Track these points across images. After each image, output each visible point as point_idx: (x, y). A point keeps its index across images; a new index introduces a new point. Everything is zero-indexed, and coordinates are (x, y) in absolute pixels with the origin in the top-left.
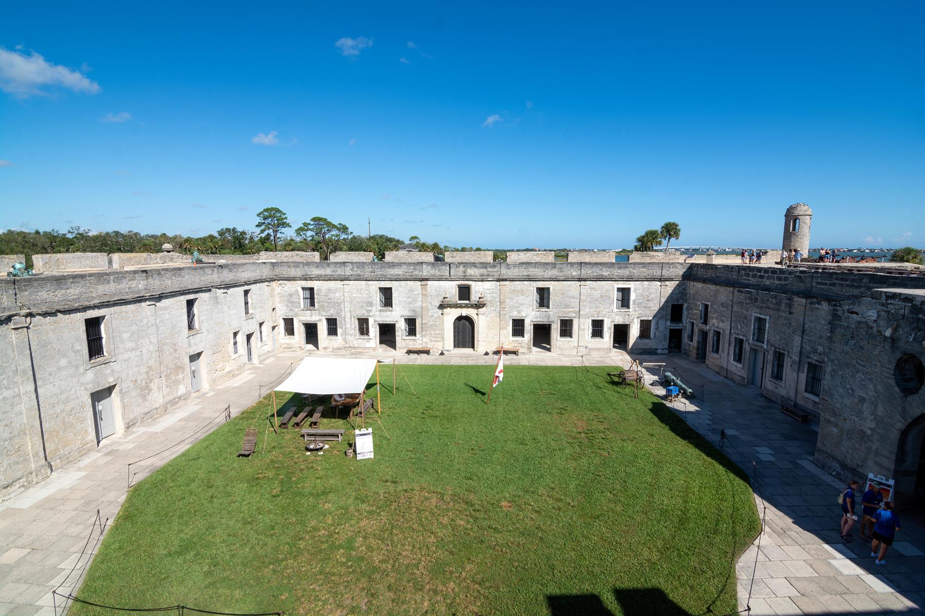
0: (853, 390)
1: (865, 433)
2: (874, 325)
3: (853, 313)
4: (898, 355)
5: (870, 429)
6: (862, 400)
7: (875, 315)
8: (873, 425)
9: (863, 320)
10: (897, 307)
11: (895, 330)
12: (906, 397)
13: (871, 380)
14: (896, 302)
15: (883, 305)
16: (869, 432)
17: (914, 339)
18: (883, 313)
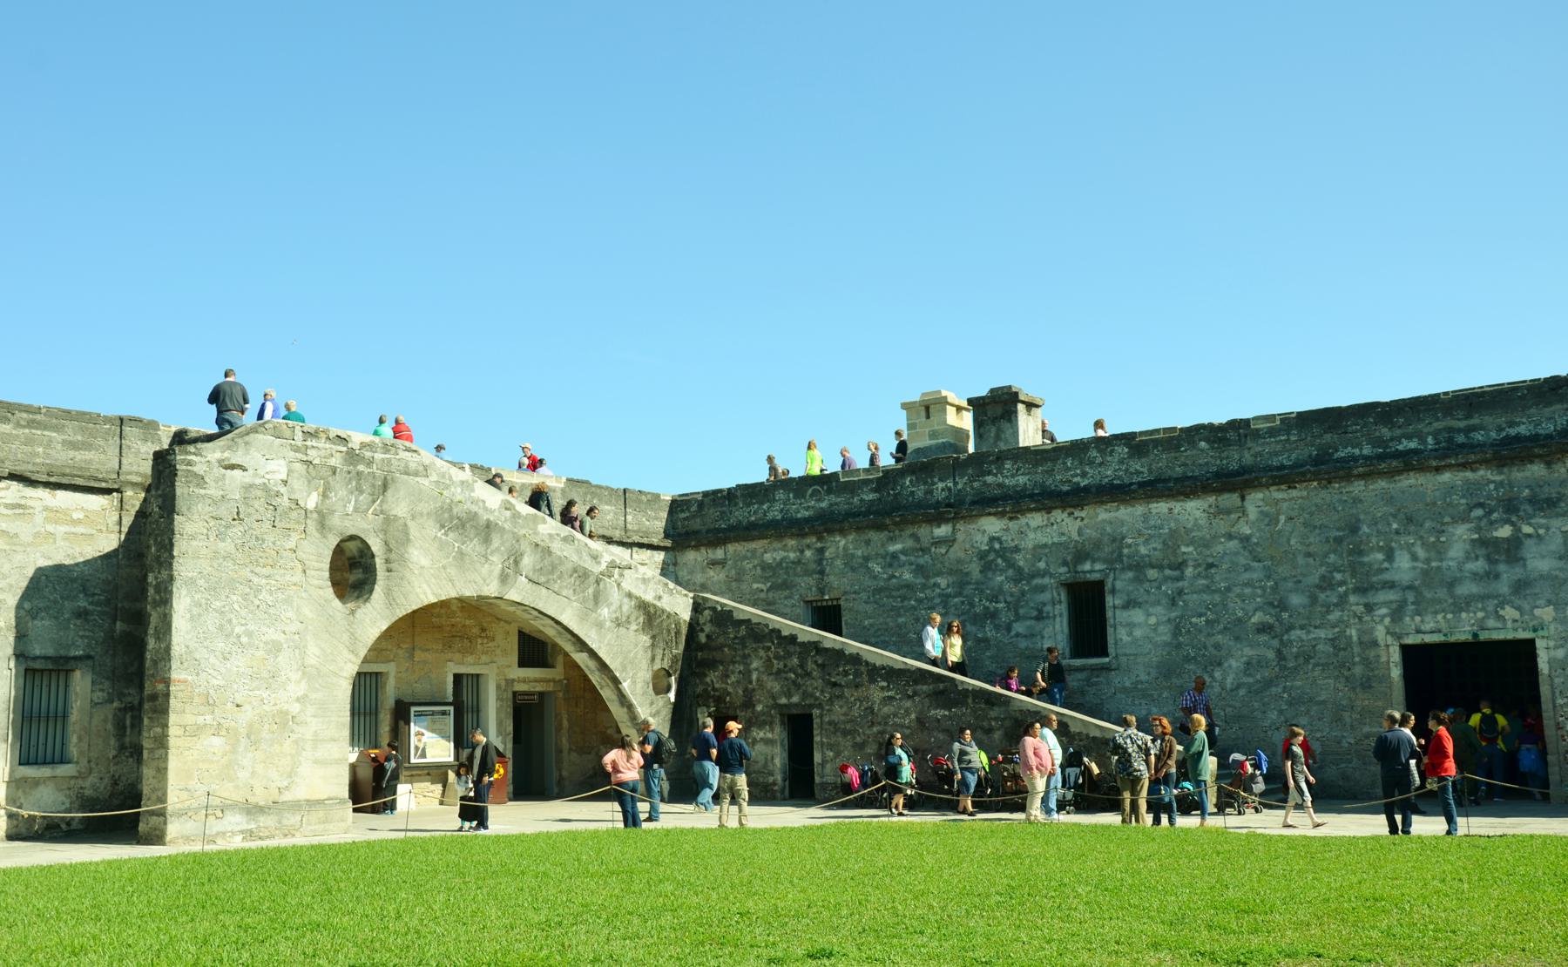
0: (249, 634)
1: (287, 713)
2: (283, 490)
3: (232, 467)
4: (333, 541)
5: (298, 700)
6: (275, 648)
7: (284, 470)
8: (301, 689)
9: (258, 481)
10: (323, 453)
11: (325, 496)
12: (353, 612)
13: (288, 601)
14: (321, 443)
15: (297, 450)
16: (295, 708)
17: (356, 510)
18: (298, 466)
